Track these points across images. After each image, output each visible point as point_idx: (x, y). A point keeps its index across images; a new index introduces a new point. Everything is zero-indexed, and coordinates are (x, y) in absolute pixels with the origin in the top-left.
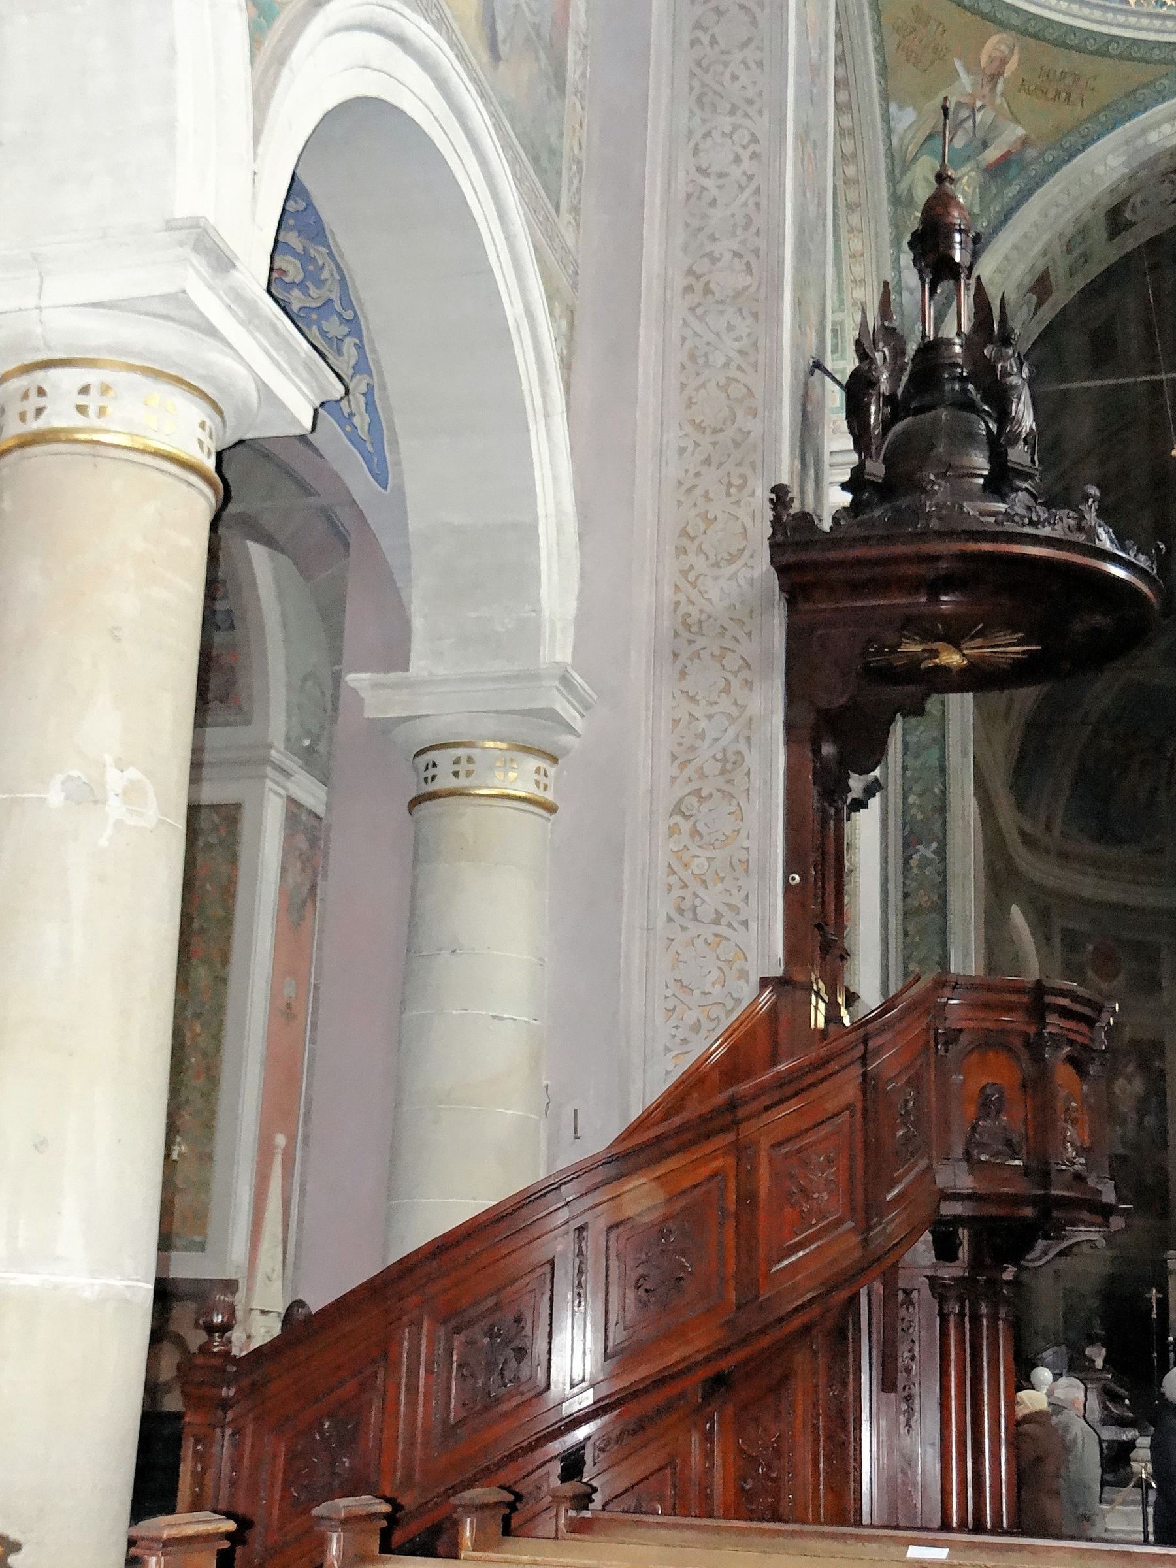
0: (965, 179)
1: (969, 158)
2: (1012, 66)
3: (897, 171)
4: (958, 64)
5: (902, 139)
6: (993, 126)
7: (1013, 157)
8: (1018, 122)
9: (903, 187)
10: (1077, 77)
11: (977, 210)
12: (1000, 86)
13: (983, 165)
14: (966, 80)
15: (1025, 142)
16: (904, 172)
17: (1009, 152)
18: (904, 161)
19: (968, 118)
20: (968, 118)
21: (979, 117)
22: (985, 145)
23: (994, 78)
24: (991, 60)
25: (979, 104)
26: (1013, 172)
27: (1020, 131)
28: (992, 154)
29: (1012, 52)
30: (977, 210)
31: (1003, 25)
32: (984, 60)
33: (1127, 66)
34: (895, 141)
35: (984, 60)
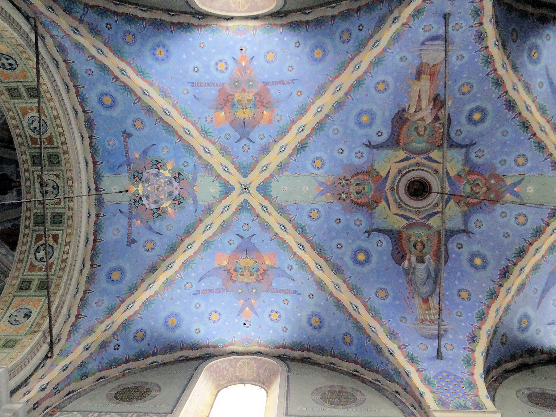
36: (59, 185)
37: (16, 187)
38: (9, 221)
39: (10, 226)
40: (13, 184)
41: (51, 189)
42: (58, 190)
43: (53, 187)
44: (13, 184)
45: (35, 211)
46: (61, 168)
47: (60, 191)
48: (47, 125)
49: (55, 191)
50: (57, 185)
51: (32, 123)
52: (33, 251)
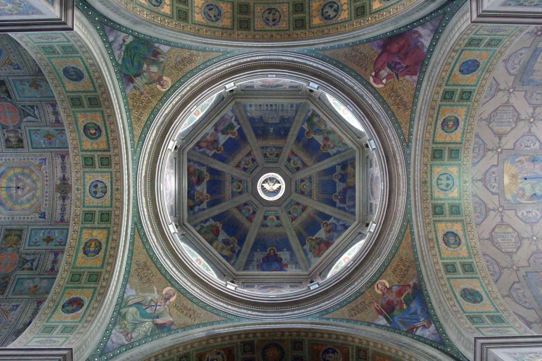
0: (147, 323)
1: (151, 317)
2: (173, 299)
3: (123, 305)
4: (155, 289)
5: (128, 297)
6: (162, 313)
7: (166, 325)
8: (171, 316)
9: (123, 311)
10: (194, 312)
11: (149, 334)
12: (168, 303)
13: (155, 323)
14: (156, 295)
15: (172, 323)
16: (125, 307)
17: (165, 323)
18: (126, 304)
19: (154, 306)
20: (154, 306)
21: (158, 307)
22: (158, 317)
23: (167, 299)
24: (166, 294)
25: (159, 304)
26: (165, 330)
27: (171, 319)
28: (159, 321)
29: (174, 295)
30: (149, 334)
31: (172, 286)
32: (164, 292)
33: (210, 314)
34: (125, 296)
35: (164, 292)
36: (266, 8)
37: (274, 251)
38: (306, 255)
39: (311, 253)
40: (272, 254)
41: (271, 15)
42: (271, 9)
43: (269, 13)
44: (272, 254)
45: (291, 29)
46: (252, 4)
47: (273, 7)
48: (212, 5)
49: (273, 11)
50: (268, 9)
51: (210, 17)
52: (329, 22)
